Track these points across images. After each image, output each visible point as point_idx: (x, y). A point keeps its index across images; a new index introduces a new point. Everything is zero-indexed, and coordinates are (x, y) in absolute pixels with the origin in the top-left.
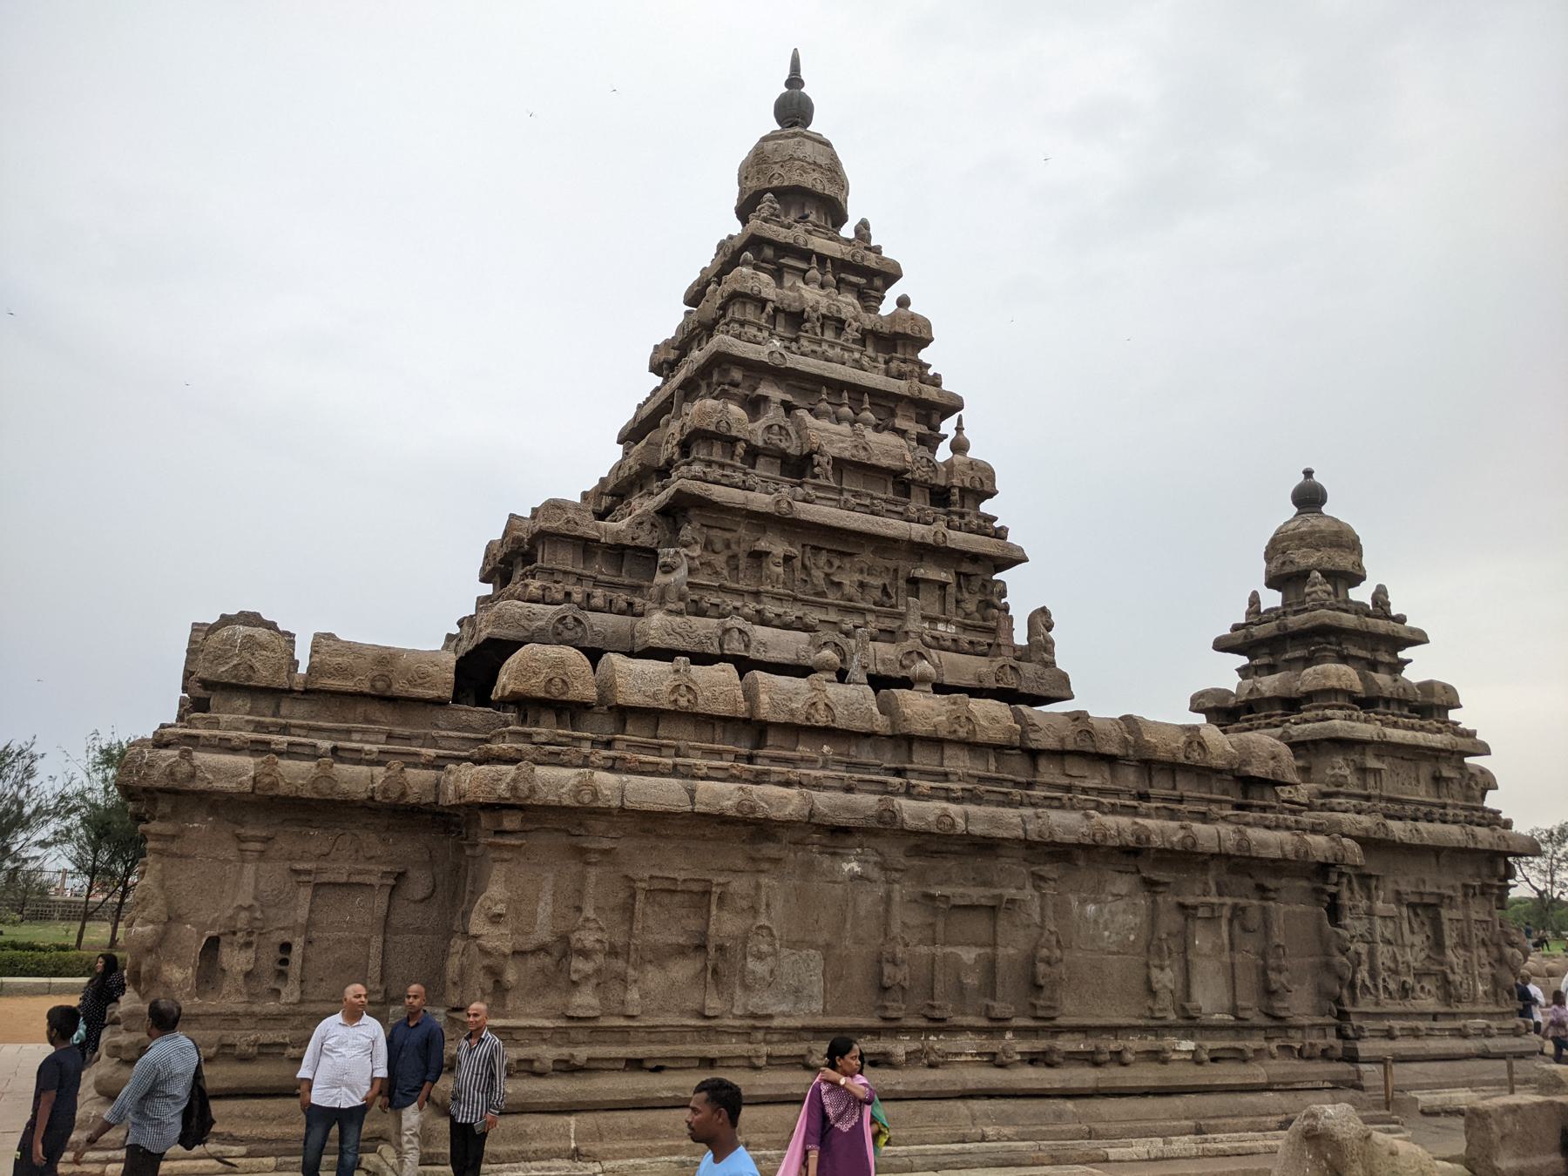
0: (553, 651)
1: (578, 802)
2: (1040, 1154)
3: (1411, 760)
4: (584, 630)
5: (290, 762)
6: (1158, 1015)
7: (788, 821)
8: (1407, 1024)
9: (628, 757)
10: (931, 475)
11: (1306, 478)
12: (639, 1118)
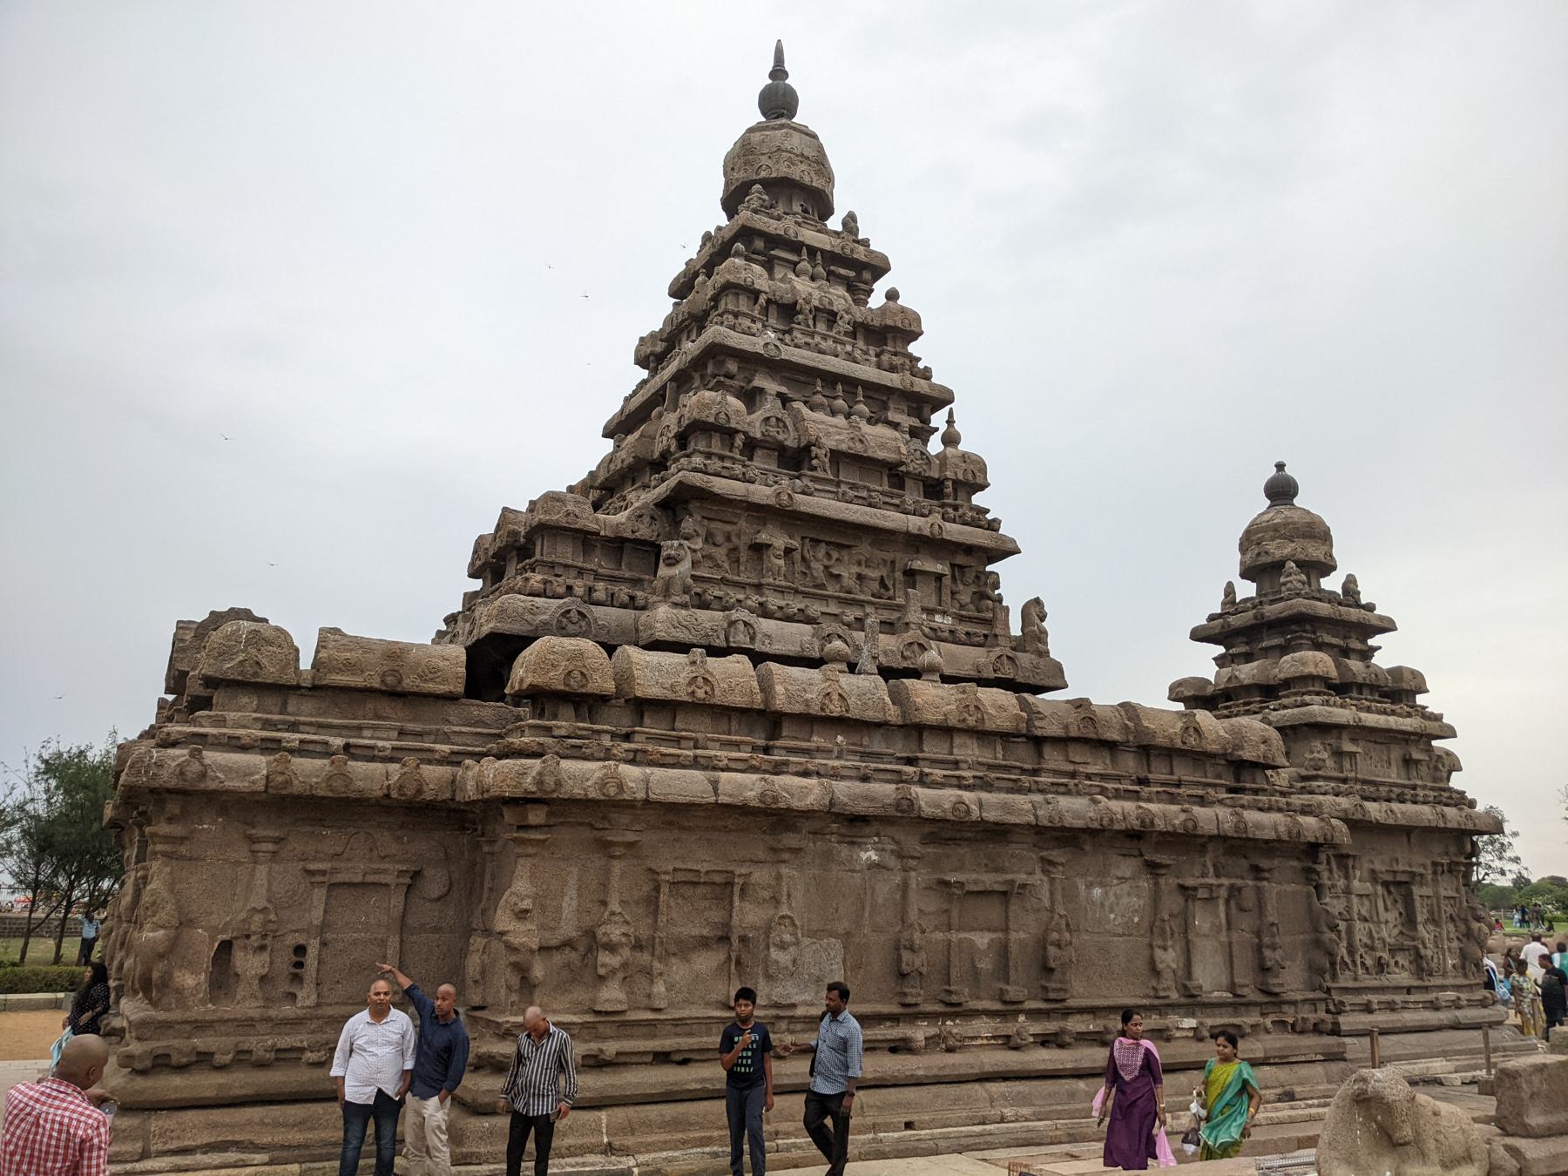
0: (569, 643)
1: (604, 794)
2: (1058, 1133)
3: (1382, 743)
4: (589, 624)
5: (303, 760)
6: (1162, 994)
7: (809, 811)
8: (1384, 998)
9: (650, 749)
10: (925, 467)
11: (1278, 471)
12: (669, 1110)
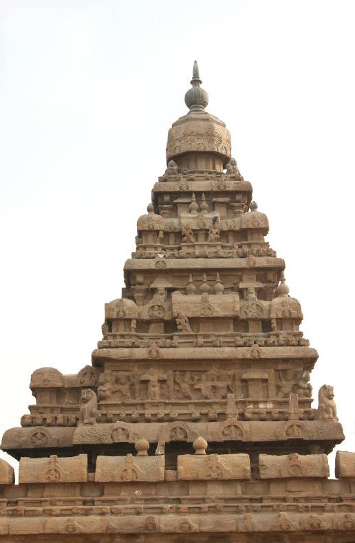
4: (47, 438)
